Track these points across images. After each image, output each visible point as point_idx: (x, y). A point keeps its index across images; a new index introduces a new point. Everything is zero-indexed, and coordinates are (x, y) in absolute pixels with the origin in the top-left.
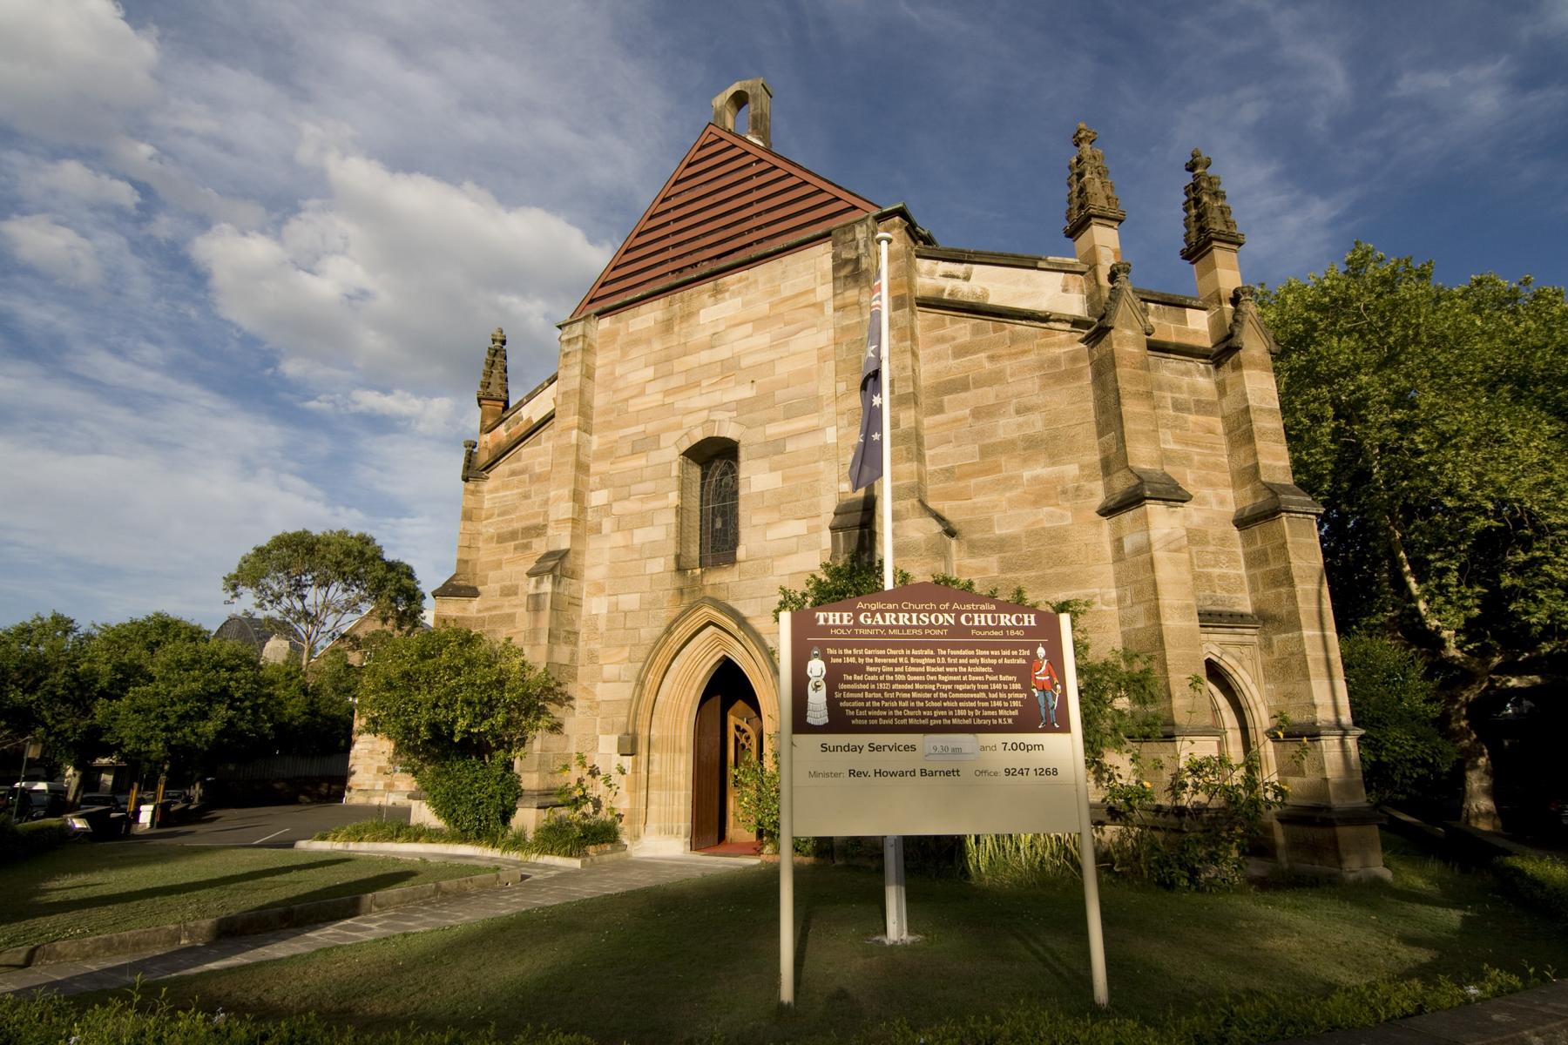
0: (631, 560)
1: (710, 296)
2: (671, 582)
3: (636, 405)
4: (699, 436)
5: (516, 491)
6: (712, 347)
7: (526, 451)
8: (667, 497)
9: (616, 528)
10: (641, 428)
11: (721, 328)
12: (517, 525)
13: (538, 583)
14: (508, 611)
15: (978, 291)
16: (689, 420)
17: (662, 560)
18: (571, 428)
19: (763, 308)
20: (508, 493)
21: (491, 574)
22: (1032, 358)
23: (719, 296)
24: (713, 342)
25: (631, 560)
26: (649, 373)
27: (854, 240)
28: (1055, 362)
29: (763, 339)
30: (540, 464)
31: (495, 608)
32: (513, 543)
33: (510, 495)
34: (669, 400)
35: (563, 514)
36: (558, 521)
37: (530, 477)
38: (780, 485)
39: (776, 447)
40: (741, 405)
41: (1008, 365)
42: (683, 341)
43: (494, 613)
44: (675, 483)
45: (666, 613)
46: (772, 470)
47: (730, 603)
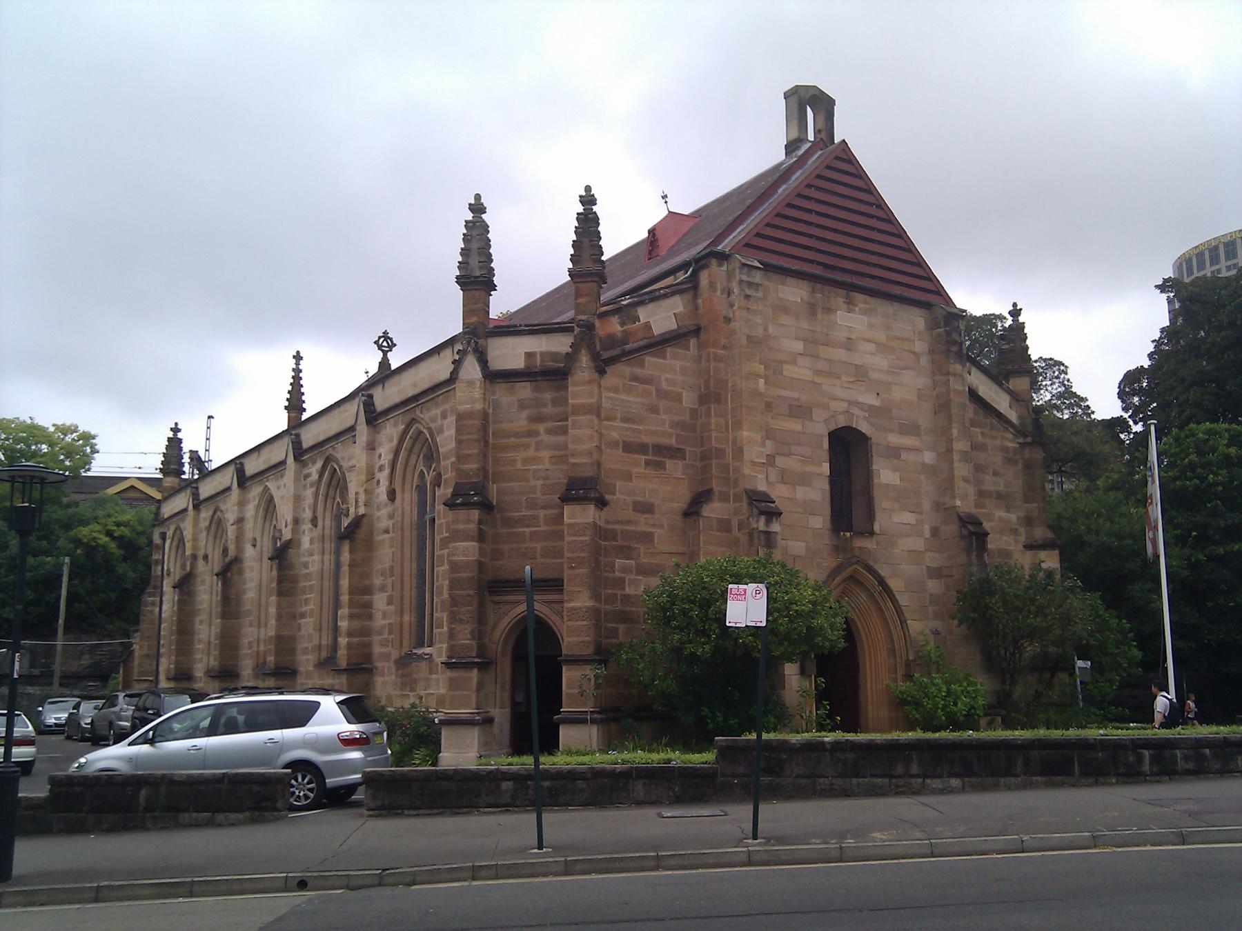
0: (796, 513)
1: (844, 302)
2: (827, 540)
3: (788, 370)
4: (842, 422)
5: (639, 400)
6: (850, 350)
7: (651, 361)
8: (821, 465)
9: (780, 479)
10: (795, 395)
11: (853, 336)
12: (649, 440)
13: (768, 522)
14: (642, 528)
15: (975, 386)
16: (834, 405)
17: (821, 519)
18: (758, 376)
19: (881, 336)
20: (631, 399)
21: (619, 484)
22: (998, 442)
23: (851, 307)
24: (849, 345)
25: (796, 513)
26: (799, 346)
27: (958, 327)
28: (1005, 450)
29: (881, 362)
30: (667, 380)
31: (628, 522)
32: (643, 457)
33: (634, 401)
34: (817, 380)
35: (757, 457)
36: (754, 464)
37: (658, 391)
38: (899, 483)
39: (894, 453)
40: (870, 409)
41: (989, 442)
42: (825, 331)
43: (628, 528)
44: (827, 457)
45: (829, 563)
46: (894, 470)
47: (872, 563)
